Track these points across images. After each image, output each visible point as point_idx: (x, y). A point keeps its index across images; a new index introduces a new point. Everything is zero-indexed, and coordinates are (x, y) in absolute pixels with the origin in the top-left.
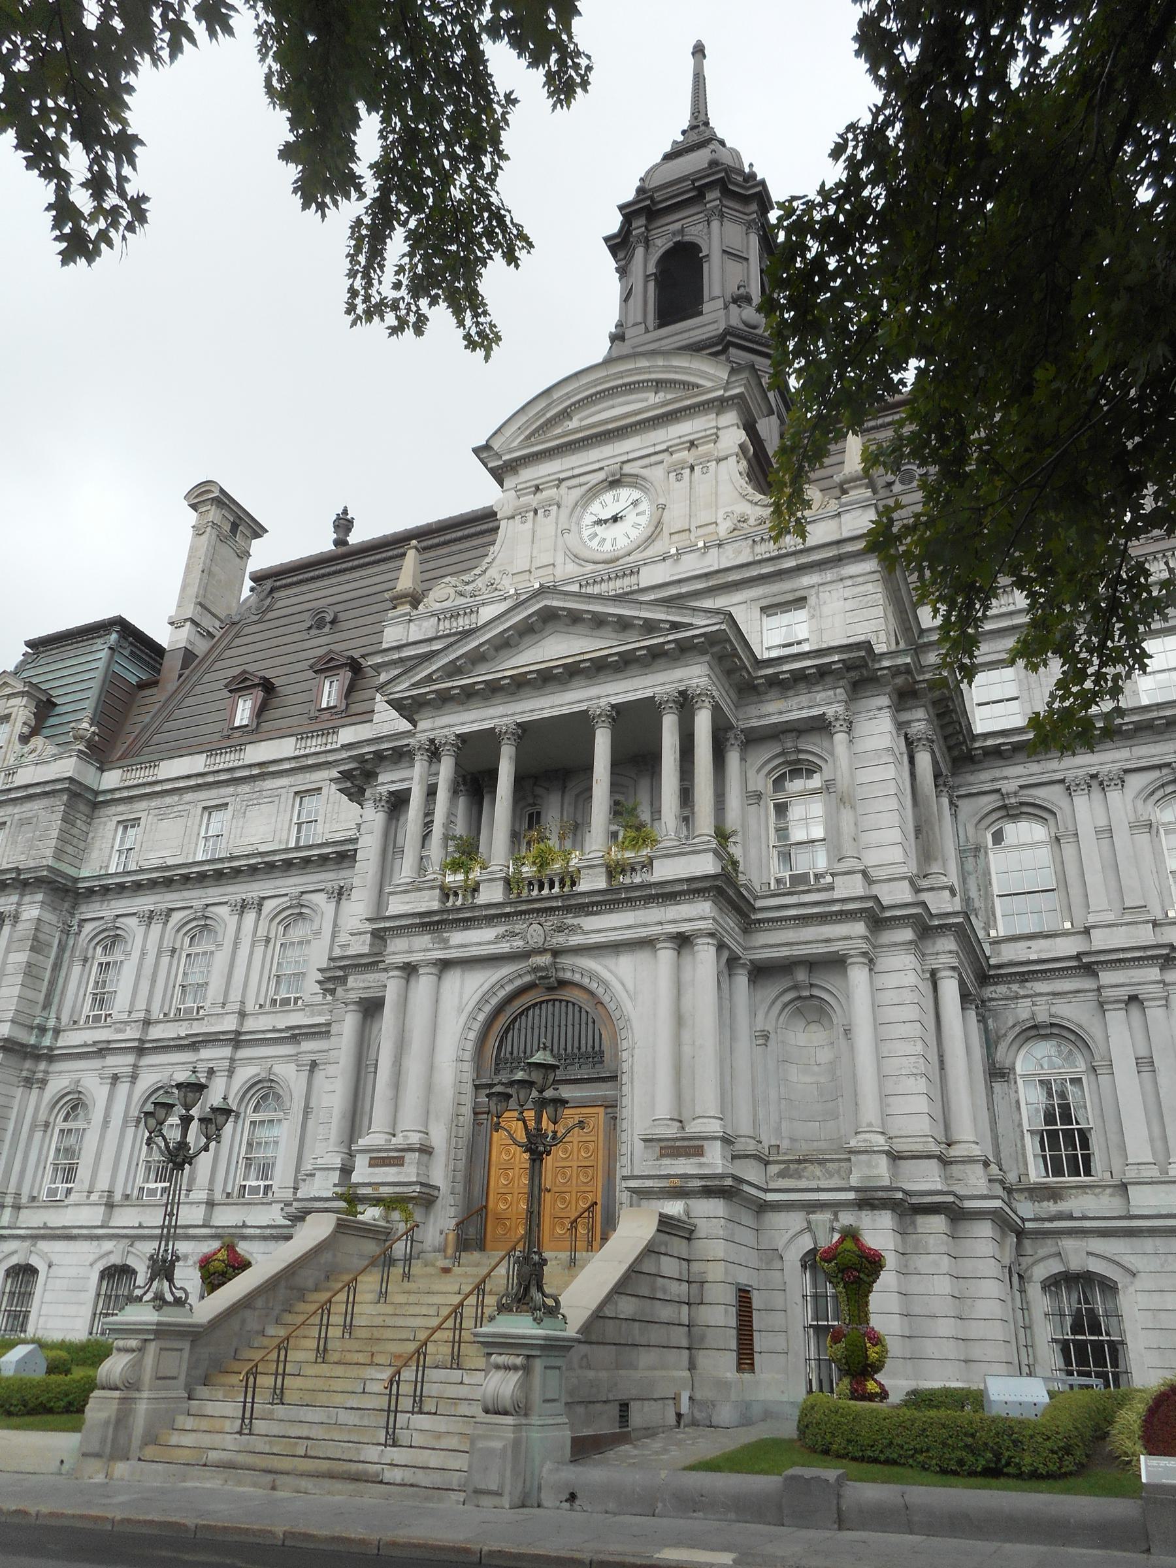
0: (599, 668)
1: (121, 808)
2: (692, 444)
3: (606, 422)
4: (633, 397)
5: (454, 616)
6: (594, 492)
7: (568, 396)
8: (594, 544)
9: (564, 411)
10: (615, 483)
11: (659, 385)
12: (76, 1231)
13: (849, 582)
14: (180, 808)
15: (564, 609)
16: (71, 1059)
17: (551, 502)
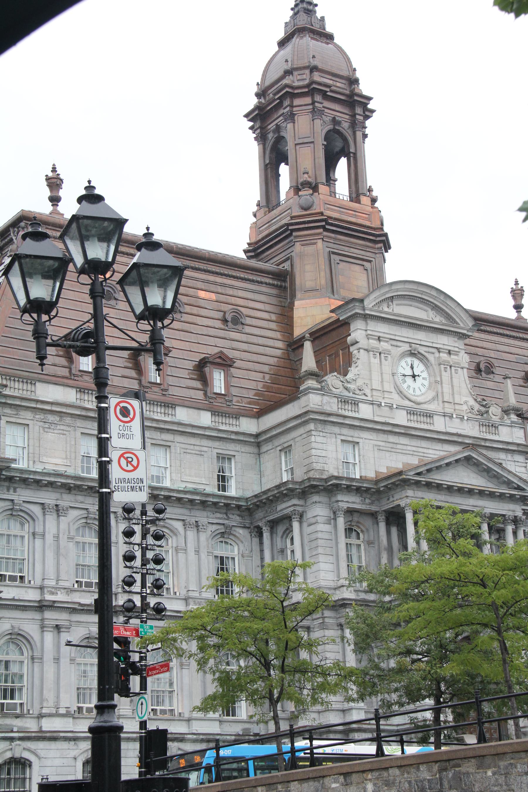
0: (491, 495)
1: (8, 411)
2: (449, 353)
3: (417, 319)
4: (421, 306)
5: (345, 401)
6: (403, 355)
7: (397, 290)
8: (405, 386)
9: (392, 297)
10: (412, 354)
11: (435, 308)
12: (62, 735)
13: (517, 464)
14: (62, 427)
15: (476, 459)
16: (12, 609)
17: (389, 353)
